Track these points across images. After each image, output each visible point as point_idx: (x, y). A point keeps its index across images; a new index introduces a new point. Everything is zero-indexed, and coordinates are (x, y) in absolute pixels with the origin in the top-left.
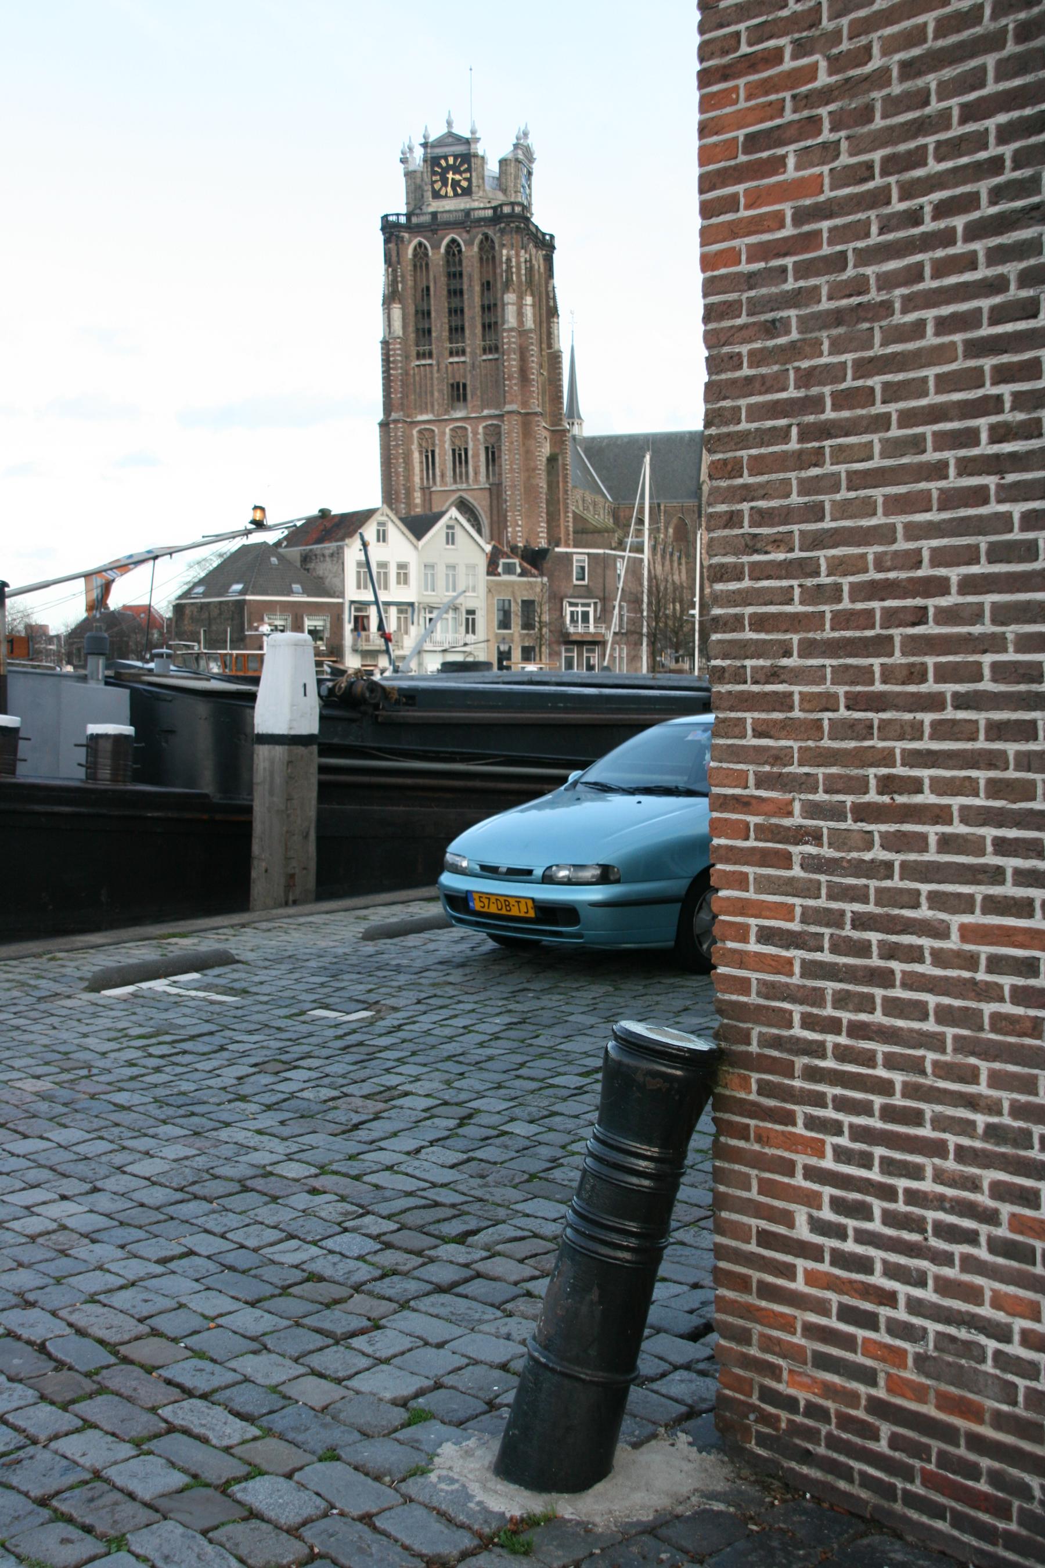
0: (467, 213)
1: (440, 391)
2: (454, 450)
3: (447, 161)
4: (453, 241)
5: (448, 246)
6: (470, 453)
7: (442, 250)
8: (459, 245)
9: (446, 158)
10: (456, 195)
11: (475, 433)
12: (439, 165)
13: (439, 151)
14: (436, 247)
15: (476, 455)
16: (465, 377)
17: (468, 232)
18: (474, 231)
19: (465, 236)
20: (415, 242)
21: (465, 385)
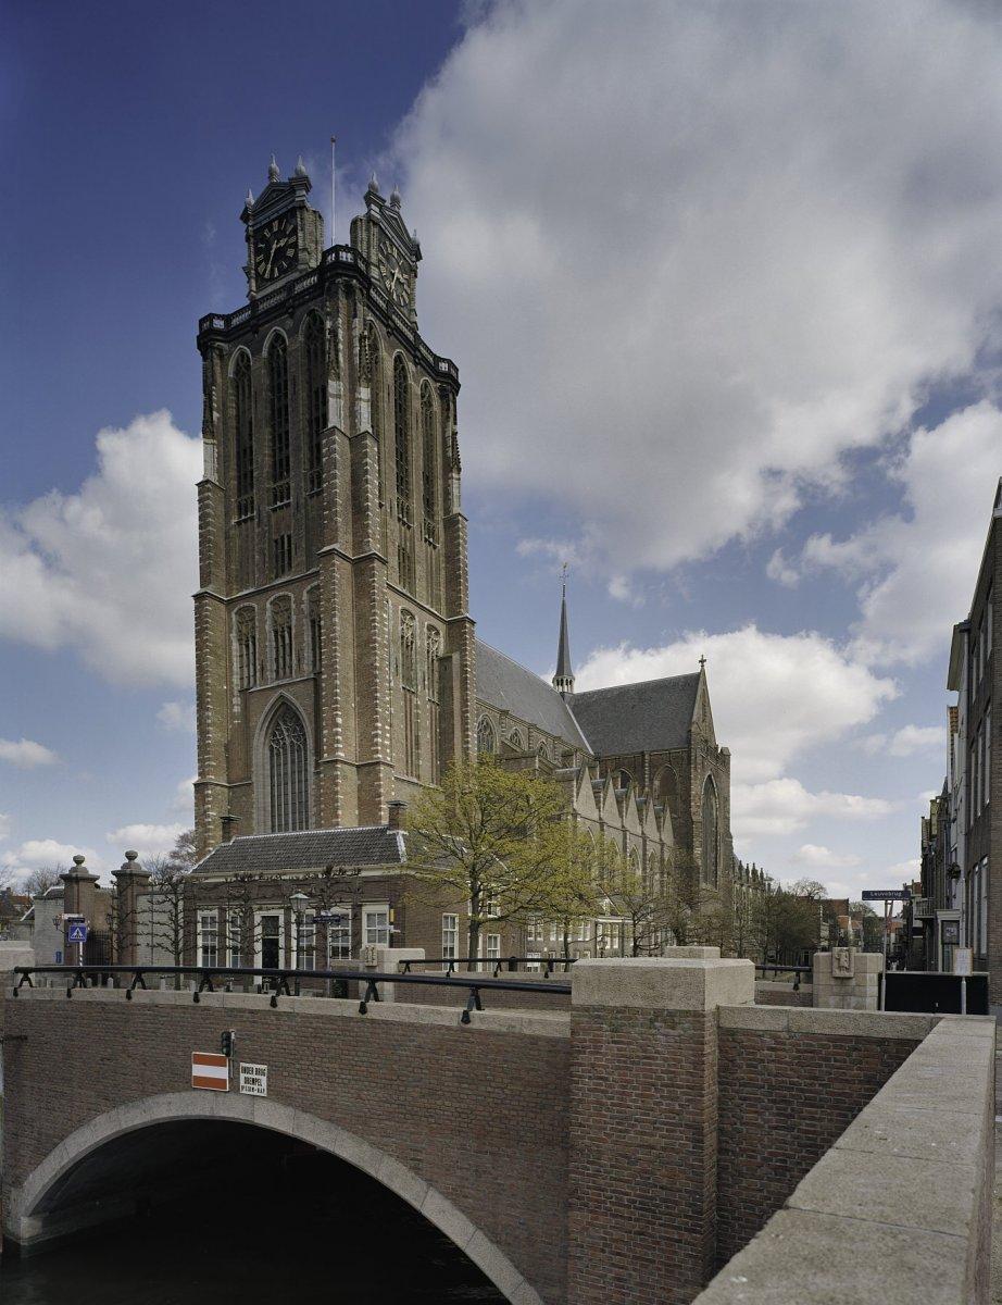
0: (290, 287)
1: (262, 552)
2: (276, 632)
3: (271, 229)
4: (278, 337)
5: (272, 347)
6: (293, 631)
7: (265, 353)
8: (284, 341)
9: (269, 225)
10: (283, 272)
11: (299, 602)
12: (263, 239)
13: (263, 219)
14: (257, 351)
15: (300, 634)
16: (289, 527)
17: (292, 316)
18: (298, 313)
19: (290, 323)
20: (236, 354)
21: (289, 537)
